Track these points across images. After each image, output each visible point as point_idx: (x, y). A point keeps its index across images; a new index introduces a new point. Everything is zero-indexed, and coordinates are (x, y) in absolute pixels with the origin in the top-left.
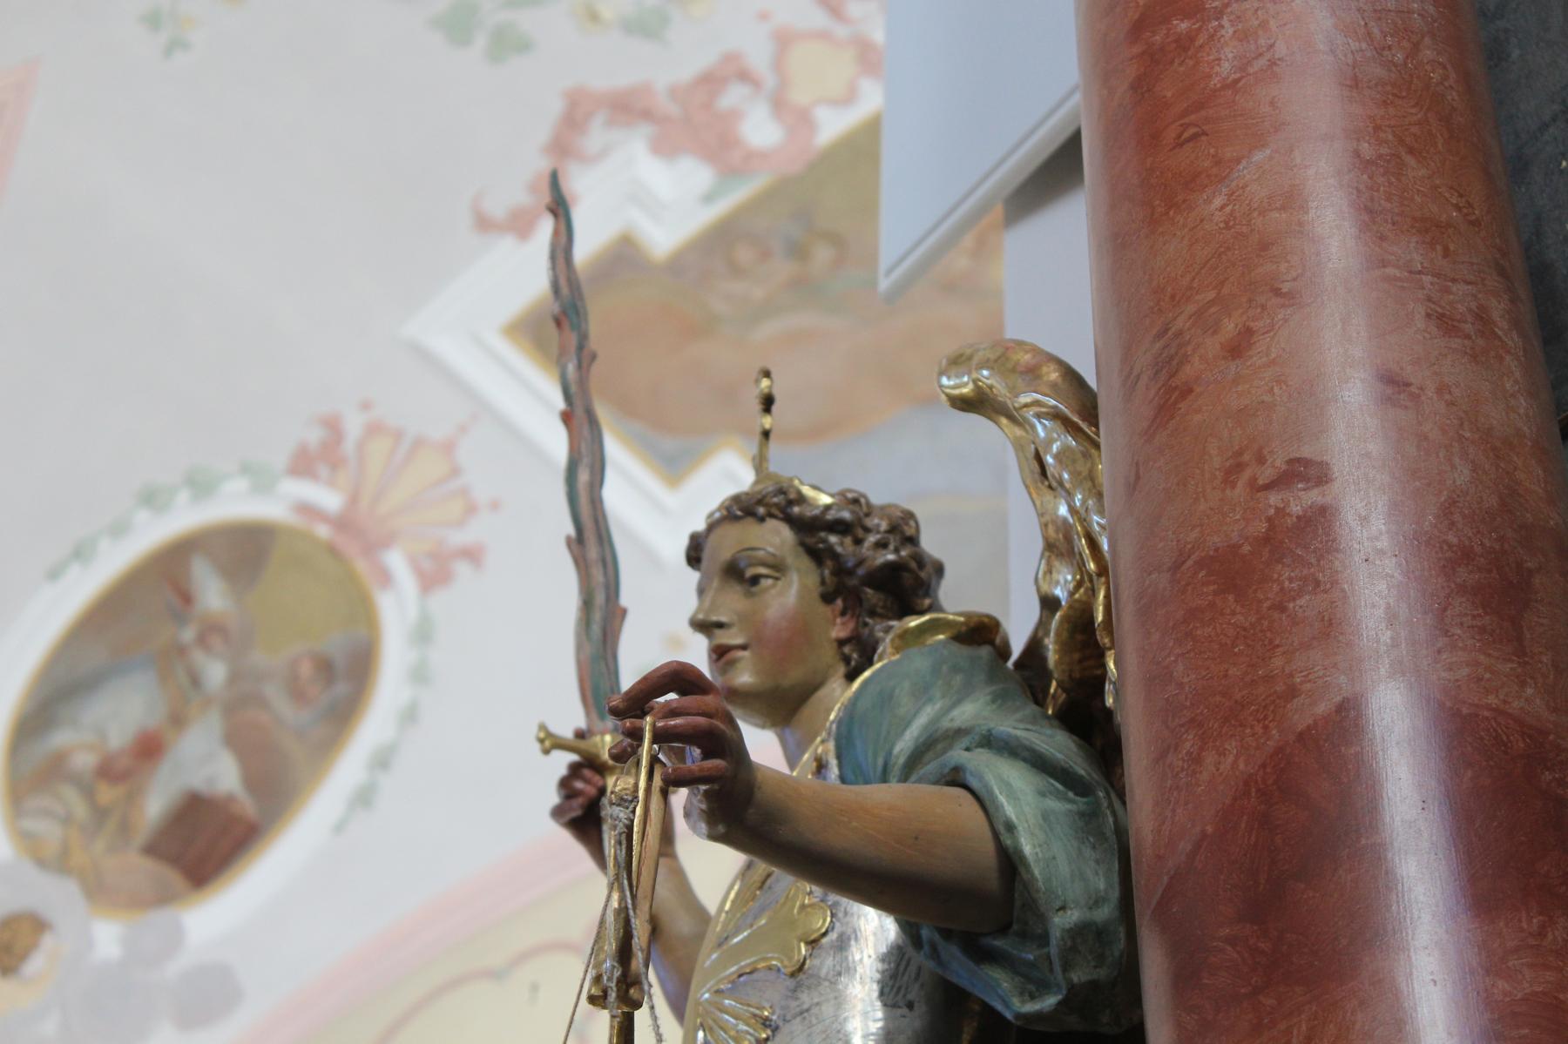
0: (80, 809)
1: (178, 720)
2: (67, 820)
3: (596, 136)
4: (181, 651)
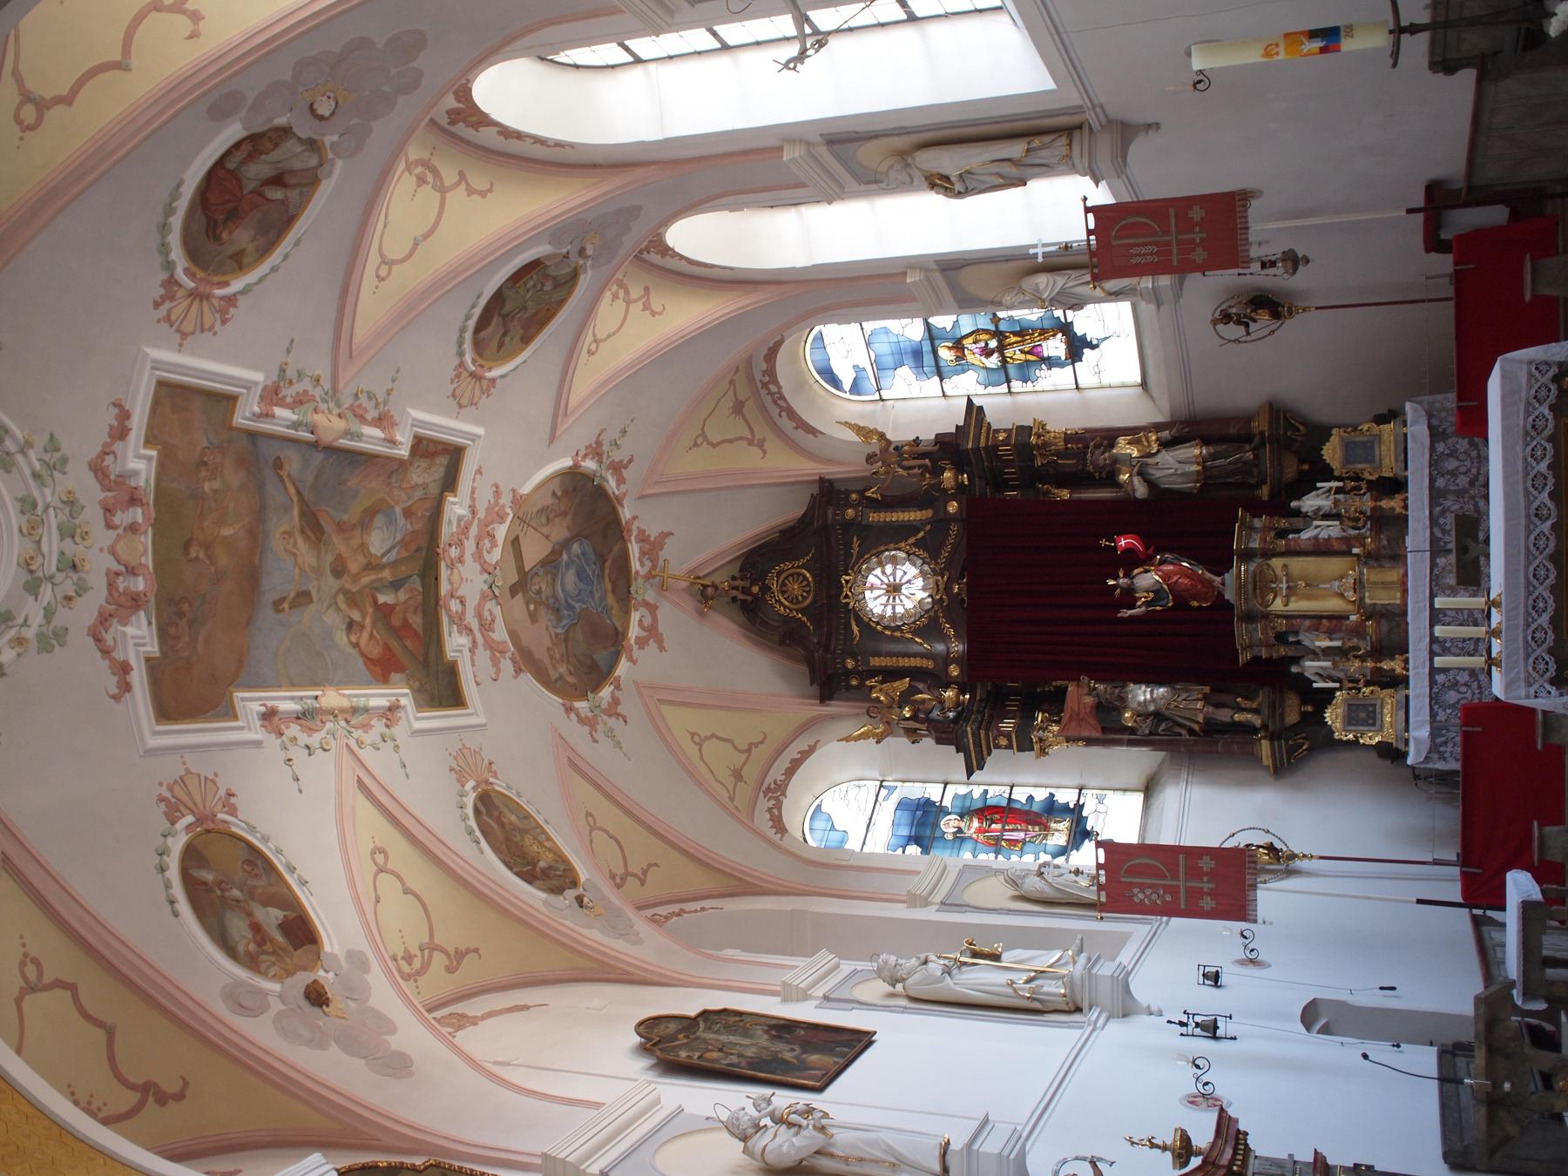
0: (273, 959)
1: (250, 914)
2: (274, 964)
3: (109, 638)
4: (223, 897)
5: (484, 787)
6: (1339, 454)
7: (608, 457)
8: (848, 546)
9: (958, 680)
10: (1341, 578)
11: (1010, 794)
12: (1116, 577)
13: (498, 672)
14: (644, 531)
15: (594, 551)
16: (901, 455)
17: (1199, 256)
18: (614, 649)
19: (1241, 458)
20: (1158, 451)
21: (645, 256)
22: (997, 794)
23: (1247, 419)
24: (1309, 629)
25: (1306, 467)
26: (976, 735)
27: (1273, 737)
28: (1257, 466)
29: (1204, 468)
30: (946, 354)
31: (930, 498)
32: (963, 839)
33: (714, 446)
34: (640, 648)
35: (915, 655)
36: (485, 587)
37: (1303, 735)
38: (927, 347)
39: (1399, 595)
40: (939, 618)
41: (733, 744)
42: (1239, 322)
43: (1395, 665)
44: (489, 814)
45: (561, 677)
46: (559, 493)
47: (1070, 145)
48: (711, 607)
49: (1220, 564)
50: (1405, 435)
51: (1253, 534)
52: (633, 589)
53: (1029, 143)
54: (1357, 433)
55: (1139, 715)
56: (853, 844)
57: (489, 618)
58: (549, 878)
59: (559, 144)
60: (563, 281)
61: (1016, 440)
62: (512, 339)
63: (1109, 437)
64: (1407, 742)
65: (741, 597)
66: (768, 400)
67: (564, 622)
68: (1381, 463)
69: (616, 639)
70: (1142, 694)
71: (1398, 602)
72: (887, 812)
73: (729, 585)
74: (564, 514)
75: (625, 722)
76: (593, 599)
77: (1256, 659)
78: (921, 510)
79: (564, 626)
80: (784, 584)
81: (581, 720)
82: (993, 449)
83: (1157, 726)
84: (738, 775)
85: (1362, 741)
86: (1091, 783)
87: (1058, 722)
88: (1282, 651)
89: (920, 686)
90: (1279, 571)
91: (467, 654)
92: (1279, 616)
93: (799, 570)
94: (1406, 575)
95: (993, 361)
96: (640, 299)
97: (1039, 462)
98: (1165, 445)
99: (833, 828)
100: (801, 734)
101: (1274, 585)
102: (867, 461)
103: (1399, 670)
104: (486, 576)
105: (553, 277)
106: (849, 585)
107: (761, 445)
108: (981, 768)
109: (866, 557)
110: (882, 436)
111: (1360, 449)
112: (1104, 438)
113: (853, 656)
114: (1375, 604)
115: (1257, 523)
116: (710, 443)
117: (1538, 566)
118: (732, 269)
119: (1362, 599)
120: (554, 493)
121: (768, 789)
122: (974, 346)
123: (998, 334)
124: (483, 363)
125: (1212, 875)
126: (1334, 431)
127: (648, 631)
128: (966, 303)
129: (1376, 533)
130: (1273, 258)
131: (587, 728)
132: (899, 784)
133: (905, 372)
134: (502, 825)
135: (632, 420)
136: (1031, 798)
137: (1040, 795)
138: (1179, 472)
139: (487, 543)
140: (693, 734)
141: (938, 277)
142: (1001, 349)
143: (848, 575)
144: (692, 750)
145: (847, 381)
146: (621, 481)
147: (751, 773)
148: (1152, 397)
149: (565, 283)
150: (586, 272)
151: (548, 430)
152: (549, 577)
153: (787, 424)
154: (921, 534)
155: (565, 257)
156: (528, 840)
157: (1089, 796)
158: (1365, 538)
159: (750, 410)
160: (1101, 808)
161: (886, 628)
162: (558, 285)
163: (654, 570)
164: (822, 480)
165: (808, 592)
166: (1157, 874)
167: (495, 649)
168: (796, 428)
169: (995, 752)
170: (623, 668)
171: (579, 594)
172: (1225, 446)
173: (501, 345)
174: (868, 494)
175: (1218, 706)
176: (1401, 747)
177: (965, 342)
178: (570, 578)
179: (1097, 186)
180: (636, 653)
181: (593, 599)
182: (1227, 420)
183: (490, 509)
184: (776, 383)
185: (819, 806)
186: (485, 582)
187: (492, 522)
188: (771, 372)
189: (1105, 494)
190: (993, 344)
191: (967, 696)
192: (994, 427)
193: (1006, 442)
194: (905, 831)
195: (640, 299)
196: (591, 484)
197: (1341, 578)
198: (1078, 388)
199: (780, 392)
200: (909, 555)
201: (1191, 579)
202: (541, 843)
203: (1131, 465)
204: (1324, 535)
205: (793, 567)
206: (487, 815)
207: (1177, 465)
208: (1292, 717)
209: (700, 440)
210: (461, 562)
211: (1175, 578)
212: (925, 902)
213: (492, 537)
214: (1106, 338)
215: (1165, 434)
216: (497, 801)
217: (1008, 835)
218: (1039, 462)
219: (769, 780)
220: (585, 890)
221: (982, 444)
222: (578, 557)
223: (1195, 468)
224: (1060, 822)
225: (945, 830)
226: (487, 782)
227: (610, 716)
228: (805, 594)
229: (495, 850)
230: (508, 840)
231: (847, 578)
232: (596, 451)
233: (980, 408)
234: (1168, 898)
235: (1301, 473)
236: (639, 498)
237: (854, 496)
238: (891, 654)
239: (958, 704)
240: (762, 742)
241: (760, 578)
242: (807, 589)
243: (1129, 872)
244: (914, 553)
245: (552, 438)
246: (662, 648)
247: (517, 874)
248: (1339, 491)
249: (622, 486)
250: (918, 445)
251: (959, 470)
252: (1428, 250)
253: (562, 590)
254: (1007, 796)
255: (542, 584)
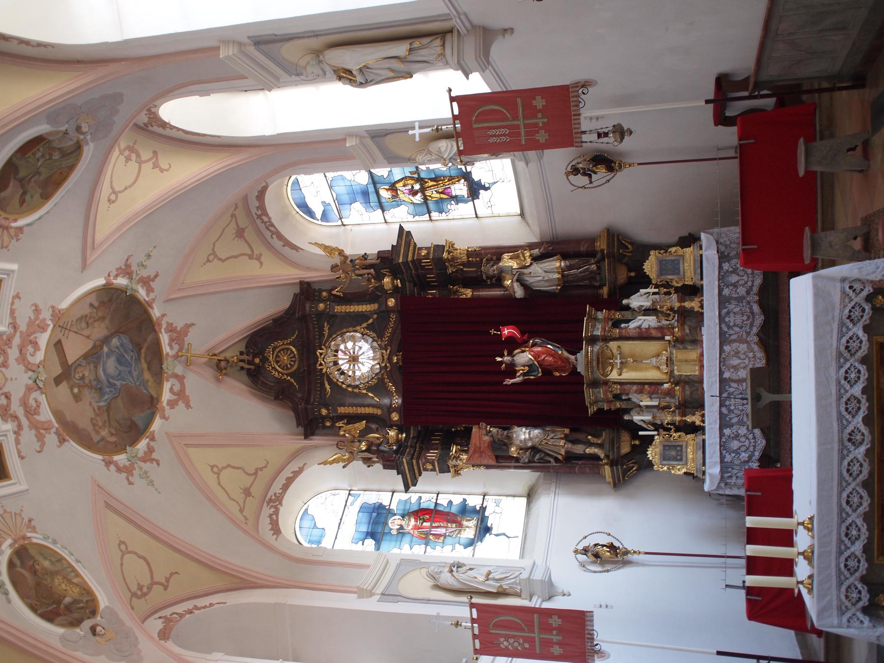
5: (21, 542)
6: (655, 268)
7: (137, 274)
8: (321, 329)
9: (399, 423)
10: (658, 355)
11: (437, 499)
12: (502, 356)
13: (43, 444)
14: (172, 324)
15: (131, 341)
16: (354, 266)
17: (542, 137)
18: (149, 411)
19: (587, 269)
20: (531, 264)
21: (150, 128)
22: (428, 501)
23: (592, 240)
24: (636, 392)
25: (633, 274)
26: (410, 464)
27: (612, 464)
28: (599, 274)
29: (562, 276)
30: (385, 194)
31: (377, 295)
32: (403, 534)
33: (223, 261)
34: (171, 408)
35: (369, 406)
36: (30, 382)
37: (634, 461)
38: (371, 189)
39: (697, 368)
40: (384, 379)
41: (243, 470)
42: (584, 174)
43: (695, 419)
44: (23, 565)
45: (103, 439)
46: (96, 304)
47: (443, 45)
48: (225, 374)
49: (575, 349)
50: (701, 256)
51: (597, 324)
52: (164, 366)
53: (411, 44)
54: (668, 254)
55: (521, 449)
56: (327, 543)
57: (34, 405)
58: (71, 612)
59: (40, 45)
60: (69, 151)
61: (434, 255)
62: (32, 197)
63: (497, 253)
64: (704, 473)
65: (246, 366)
66: (262, 227)
67: (106, 397)
68: (684, 275)
69: (151, 404)
70: (523, 435)
71: (697, 373)
72: (353, 512)
73: (237, 358)
74: (103, 319)
75: (158, 464)
76: (132, 377)
77: (600, 411)
78: (370, 304)
79: (105, 401)
80: (277, 356)
81: (119, 470)
82: (417, 263)
83: (534, 457)
84: (247, 492)
85: (673, 472)
86: (491, 491)
87: (466, 452)
88: (618, 405)
89: (374, 426)
90: (615, 351)
91: (12, 437)
92: (615, 383)
93: (287, 346)
94: (702, 355)
95: (418, 198)
96: (150, 159)
97: (450, 271)
98: (536, 259)
99: (315, 527)
100: (294, 458)
101: (611, 361)
102: (331, 270)
103: (698, 423)
104: (30, 373)
105: (59, 149)
106: (322, 356)
107: (258, 258)
108: (415, 485)
109: (334, 336)
110: (341, 253)
111: (670, 267)
112: (493, 254)
113: (326, 406)
114: (681, 375)
115: (600, 315)
116: (220, 259)
117: (851, 493)
118: (219, 137)
119: (672, 371)
120: (91, 305)
121: (270, 500)
122: (404, 188)
123: (420, 180)
124: (7, 216)
125: (560, 630)
126: (652, 252)
127: (178, 395)
128: (393, 159)
129: (681, 325)
130: (606, 130)
131: (124, 475)
132: (362, 492)
133: (358, 206)
134: (34, 572)
135: (154, 247)
136: (450, 502)
137: (457, 500)
138: (545, 279)
139: (30, 349)
140: (212, 467)
141: (369, 141)
142: (423, 190)
143: (322, 349)
144: (210, 479)
145: (318, 211)
146: (150, 290)
147: (257, 490)
148: (528, 224)
149: (72, 153)
150: (88, 144)
151: (79, 260)
152: (92, 366)
153: (277, 244)
154: (371, 321)
155: (65, 133)
156: (58, 580)
157: (490, 501)
158: (673, 328)
159: (249, 234)
160: (498, 510)
161: (349, 386)
162: (64, 154)
163: (181, 352)
164: (302, 283)
165: (294, 362)
166: (518, 628)
167: (40, 429)
168: (284, 246)
169: (424, 473)
170: (157, 425)
171: (119, 375)
172: (577, 261)
173: (22, 202)
174: (334, 292)
175: (574, 442)
176: (700, 475)
177: (397, 185)
178: (111, 364)
179: (468, 78)
180: (168, 411)
181: (132, 377)
182: (578, 241)
183: (31, 323)
184: (267, 215)
185: (306, 510)
186: (30, 378)
187: (34, 332)
188: (262, 207)
189: (496, 292)
190: (417, 187)
191: (404, 435)
192: (419, 246)
193: (426, 257)
194: (364, 528)
195: (150, 159)
196: (124, 295)
197: (658, 355)
198: (477, 217)
199: (270, 221)
200: (363, 335)
201: (554, 357)
202: (70, 581)
203: (512, 274)
204: (645, 325)
205: (283, 344)
206: (21, 567)
207: (544, 274)
208: (625, 449)
209: (211, 258)
210: (4, 366)
211: (543, 357)
212: (370, 594)
213: (35, 345)
214: (495, 183)
215: (536, 252)
216: (33, 552)
217: (434, 531)
218: (450, 270)
219: (271, 493)
220: (102, 617)
221: (410, 259)
222: (117, 348)
223: (557, 276)
224: (470, 520)
225: (392, 527)
226: (24, 538)
227: (145, 461)
228: (292, 363)
229: (23, 596)
230: (38, 584)
231: (321, 351)
232: (126, 271)
233: (409, 233)
234: (527, 646)
235: (630, 278)
236: (166, 301)
237: (324, 294)
238: (352, 405)
239: (398, 441)
240: (266, 467)
241: (260, 353)
242: (293, 359)
243: (497, 626)
244: (366, 334)
245: (84, 266)
246: (188, 406)
247: (43, 616)
248: (654, 294)
249: (151, 294)
250: (366, 259)
251: (395, 277)
252: (716, 124)
253: (104, 373)
254: (435, 501)
255: (87, 372)
